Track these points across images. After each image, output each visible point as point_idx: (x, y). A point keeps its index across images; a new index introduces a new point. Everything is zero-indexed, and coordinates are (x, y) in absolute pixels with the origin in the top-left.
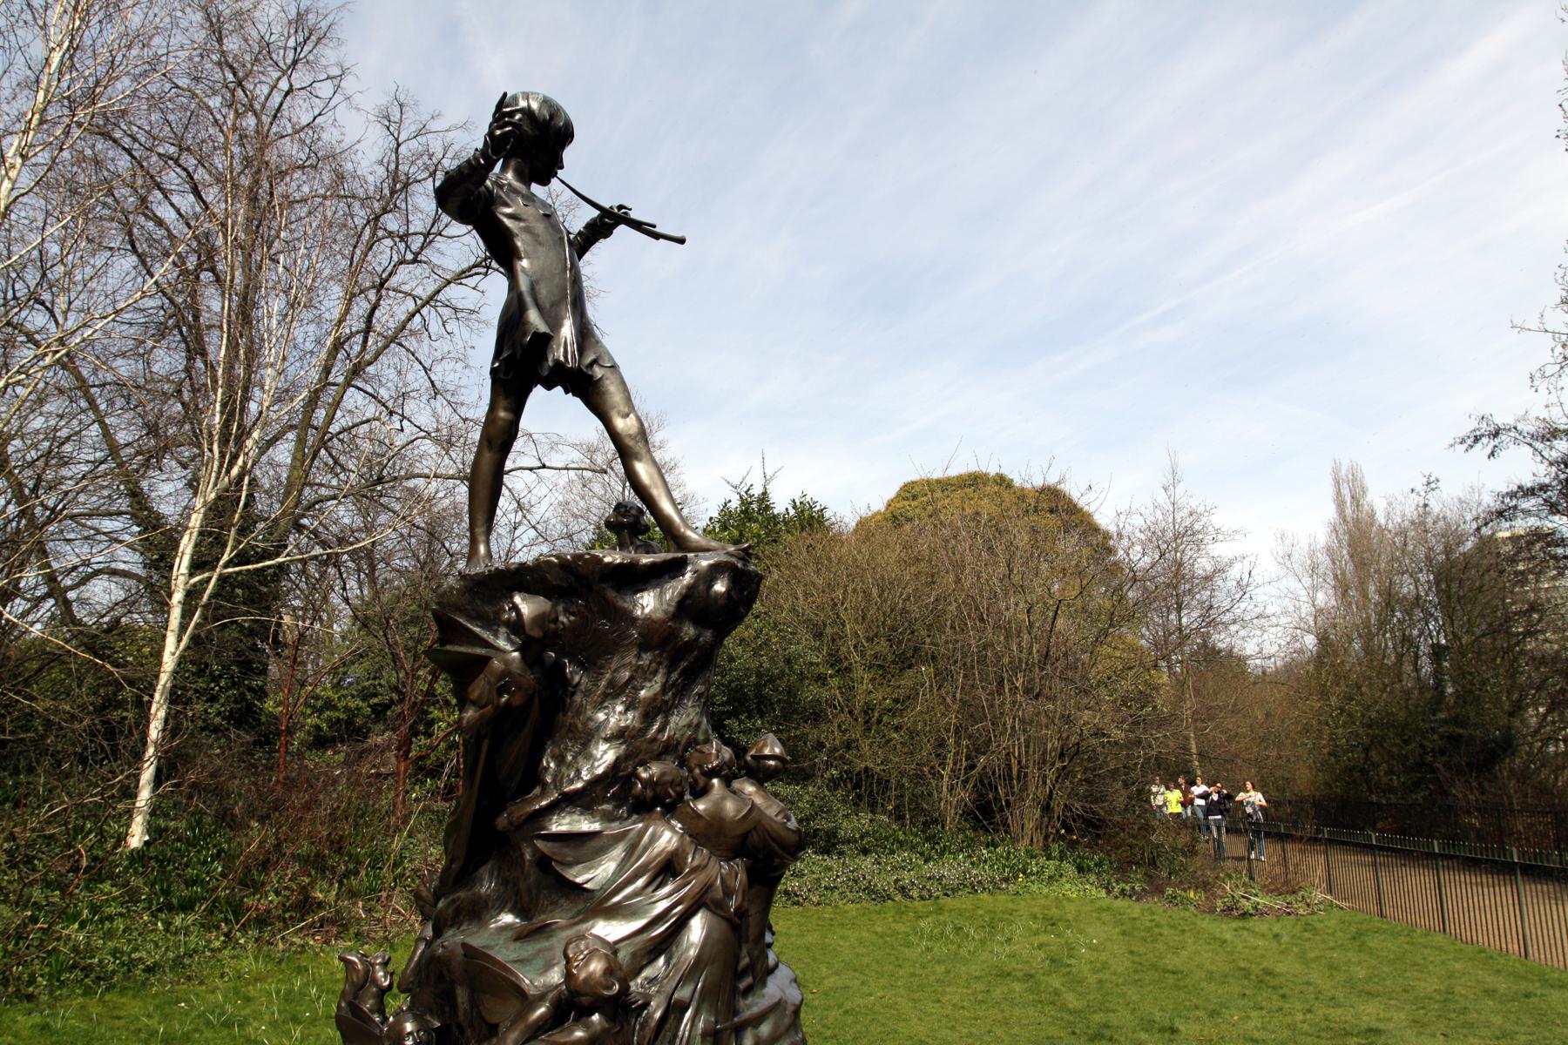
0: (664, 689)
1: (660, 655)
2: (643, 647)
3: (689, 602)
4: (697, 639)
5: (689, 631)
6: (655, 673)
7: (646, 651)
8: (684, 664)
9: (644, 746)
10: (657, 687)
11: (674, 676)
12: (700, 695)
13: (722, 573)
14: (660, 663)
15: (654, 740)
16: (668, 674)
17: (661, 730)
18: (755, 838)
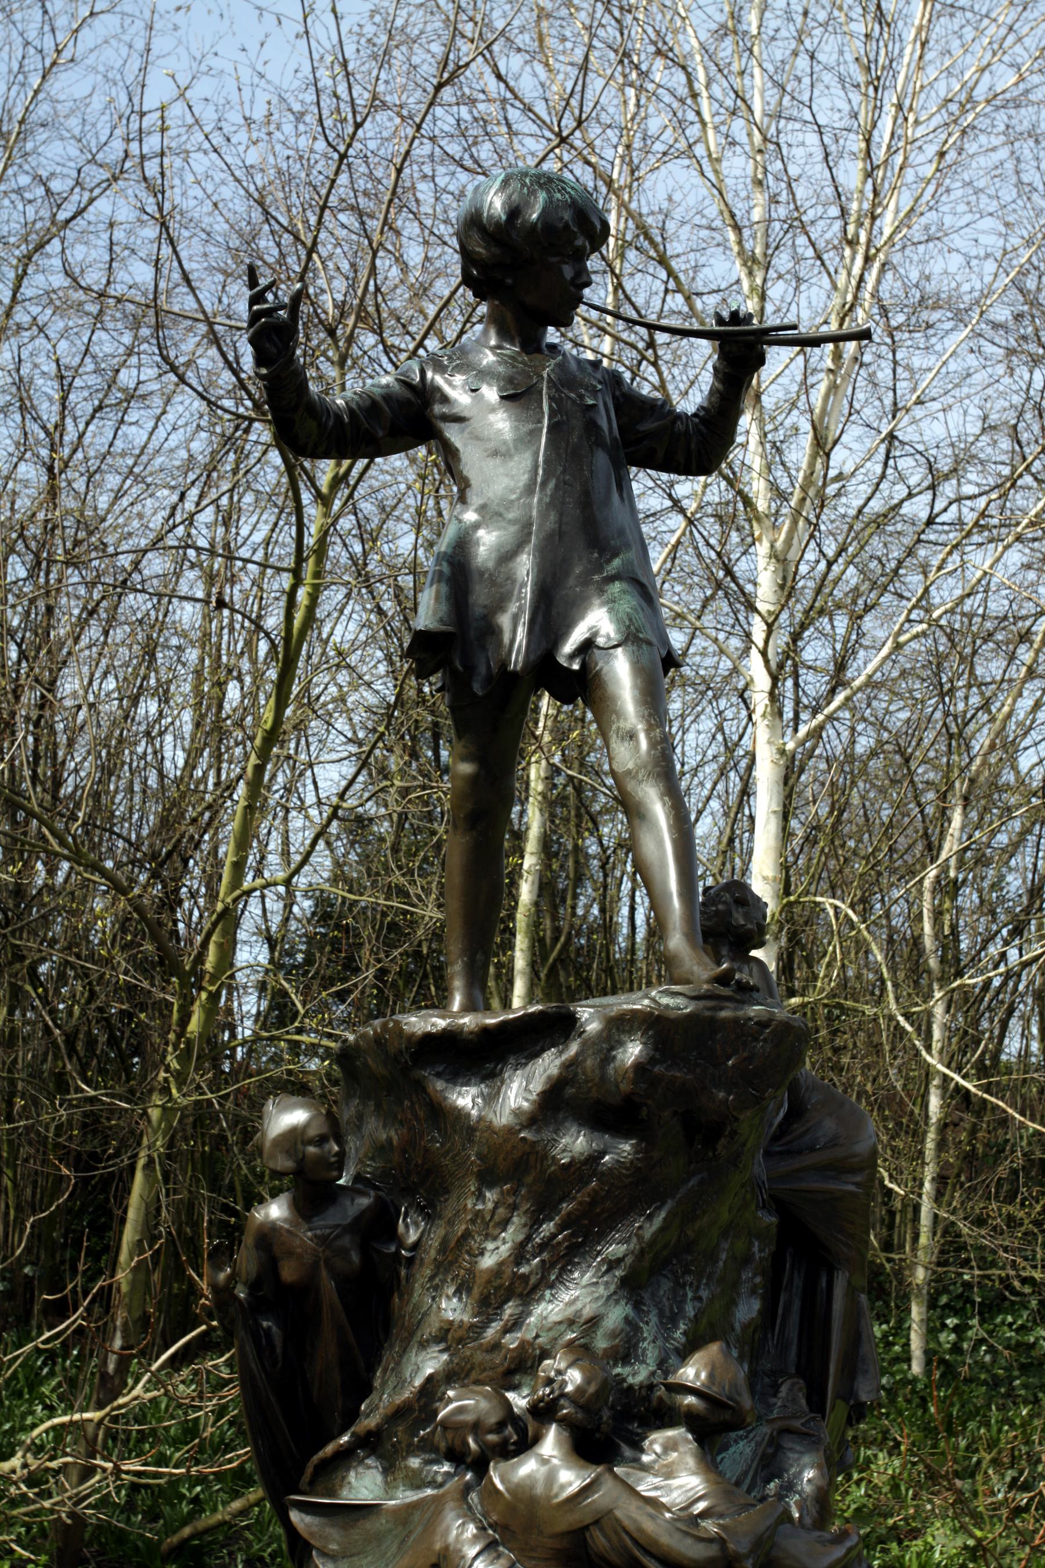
0: (519, 1255)
1: (514, 1192)
2: (487, 1178)
3: (570, 1091)
4: (594, 1158)
5: (574, 1143)
6: (504, 1224)
7: (490, 1186)
8: (566, 1207)
9: (479, 1357)
10: (505, 1250)
11: (548, 1228)
12: (612, 1264)
13: (630, 1032)
14: (514, 1207)
15: (496, 1346)
16: (534, 1224)
17: (515, 1324)
18: (599, 1540)
